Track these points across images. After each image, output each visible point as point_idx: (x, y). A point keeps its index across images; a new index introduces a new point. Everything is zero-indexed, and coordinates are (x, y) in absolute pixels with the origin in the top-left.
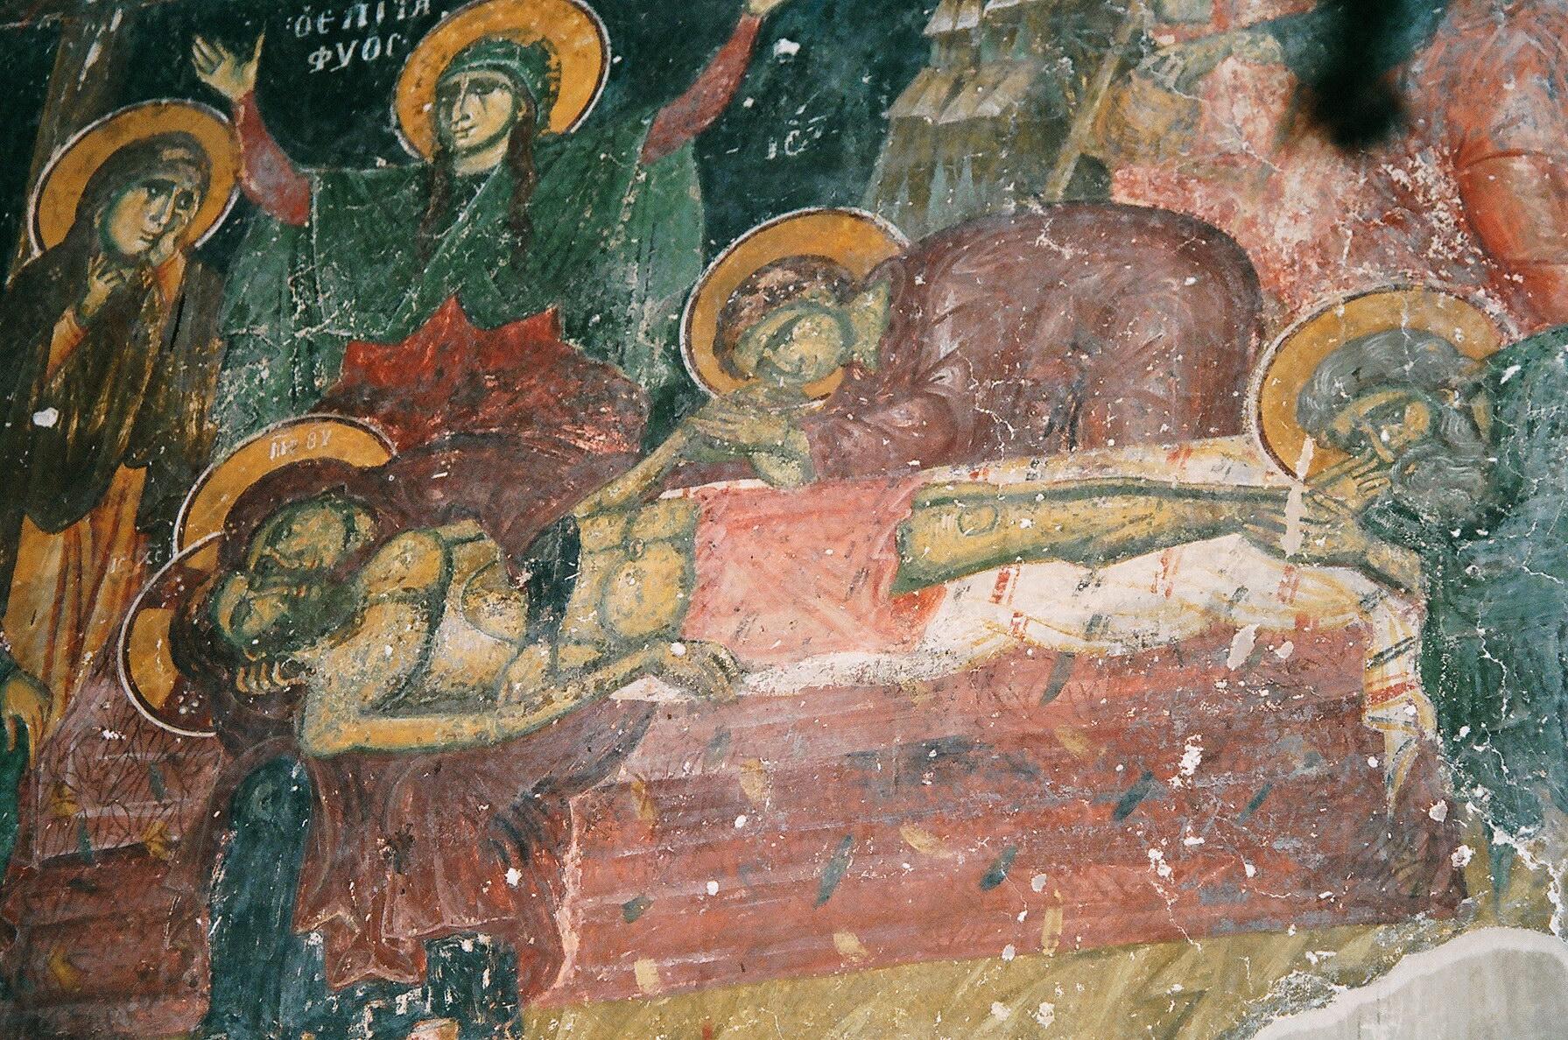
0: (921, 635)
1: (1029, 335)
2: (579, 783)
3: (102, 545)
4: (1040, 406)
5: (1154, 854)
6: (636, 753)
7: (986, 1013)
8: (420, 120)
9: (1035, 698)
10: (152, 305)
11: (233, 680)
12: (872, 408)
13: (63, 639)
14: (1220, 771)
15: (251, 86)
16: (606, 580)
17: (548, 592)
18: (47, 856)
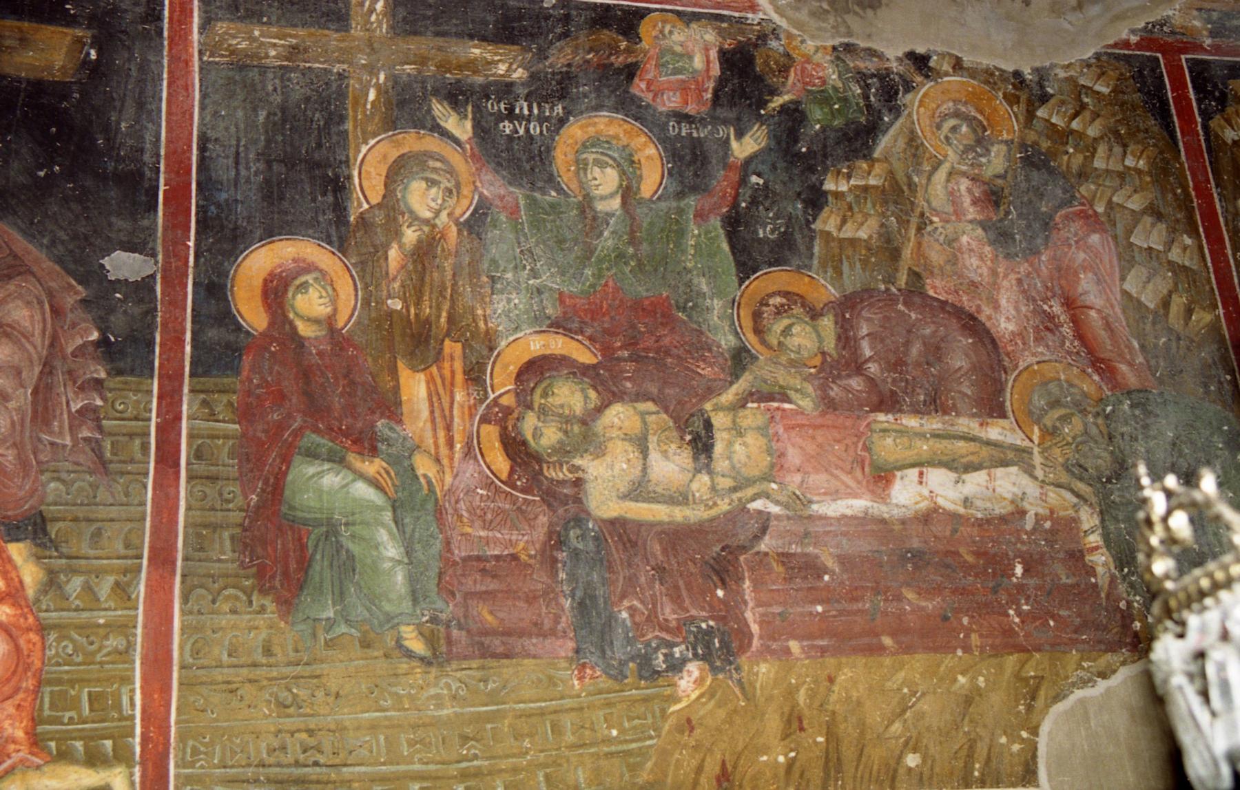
0: (889, 495)
1: (906, 353)
2: (743, 549)
3: (447, 383)
4: (918, 390)
5: (1011, 612)
6: (767, 537)
7: (955, 680)
8: (571, 174)
9: (948, 533)
10: (443, 250)
11: (541, 469)
12: (839, 377)
13: (441, 434)
14: (1032, 577)
15: (470, 134)
16: (730, 444)
17: (702, 445)
18: (463, 554)
